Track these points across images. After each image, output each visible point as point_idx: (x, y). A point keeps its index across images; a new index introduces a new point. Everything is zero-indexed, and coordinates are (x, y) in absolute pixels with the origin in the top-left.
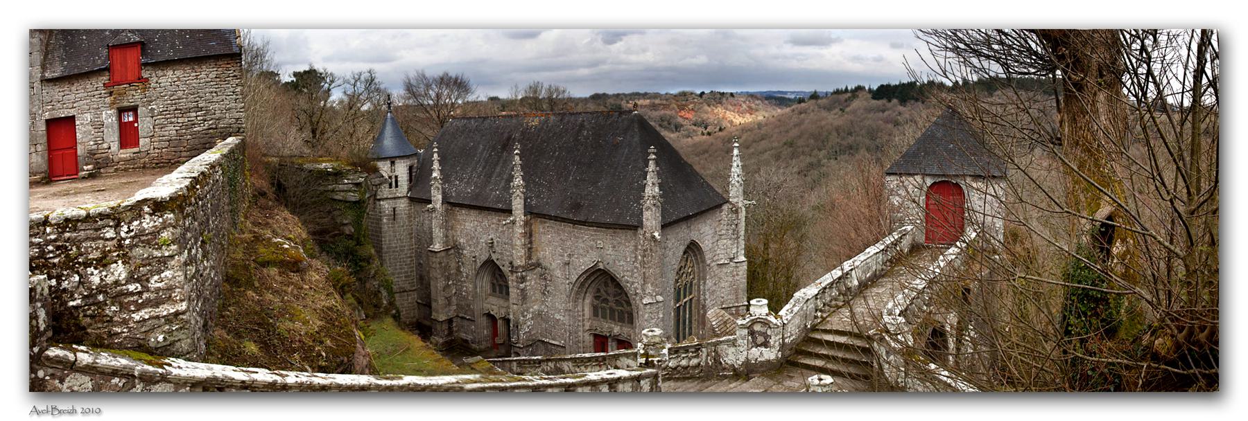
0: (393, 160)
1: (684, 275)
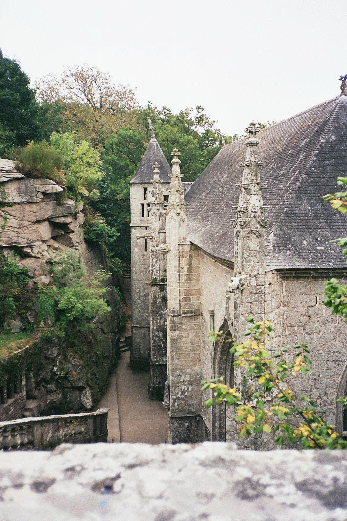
0: (146, 186)
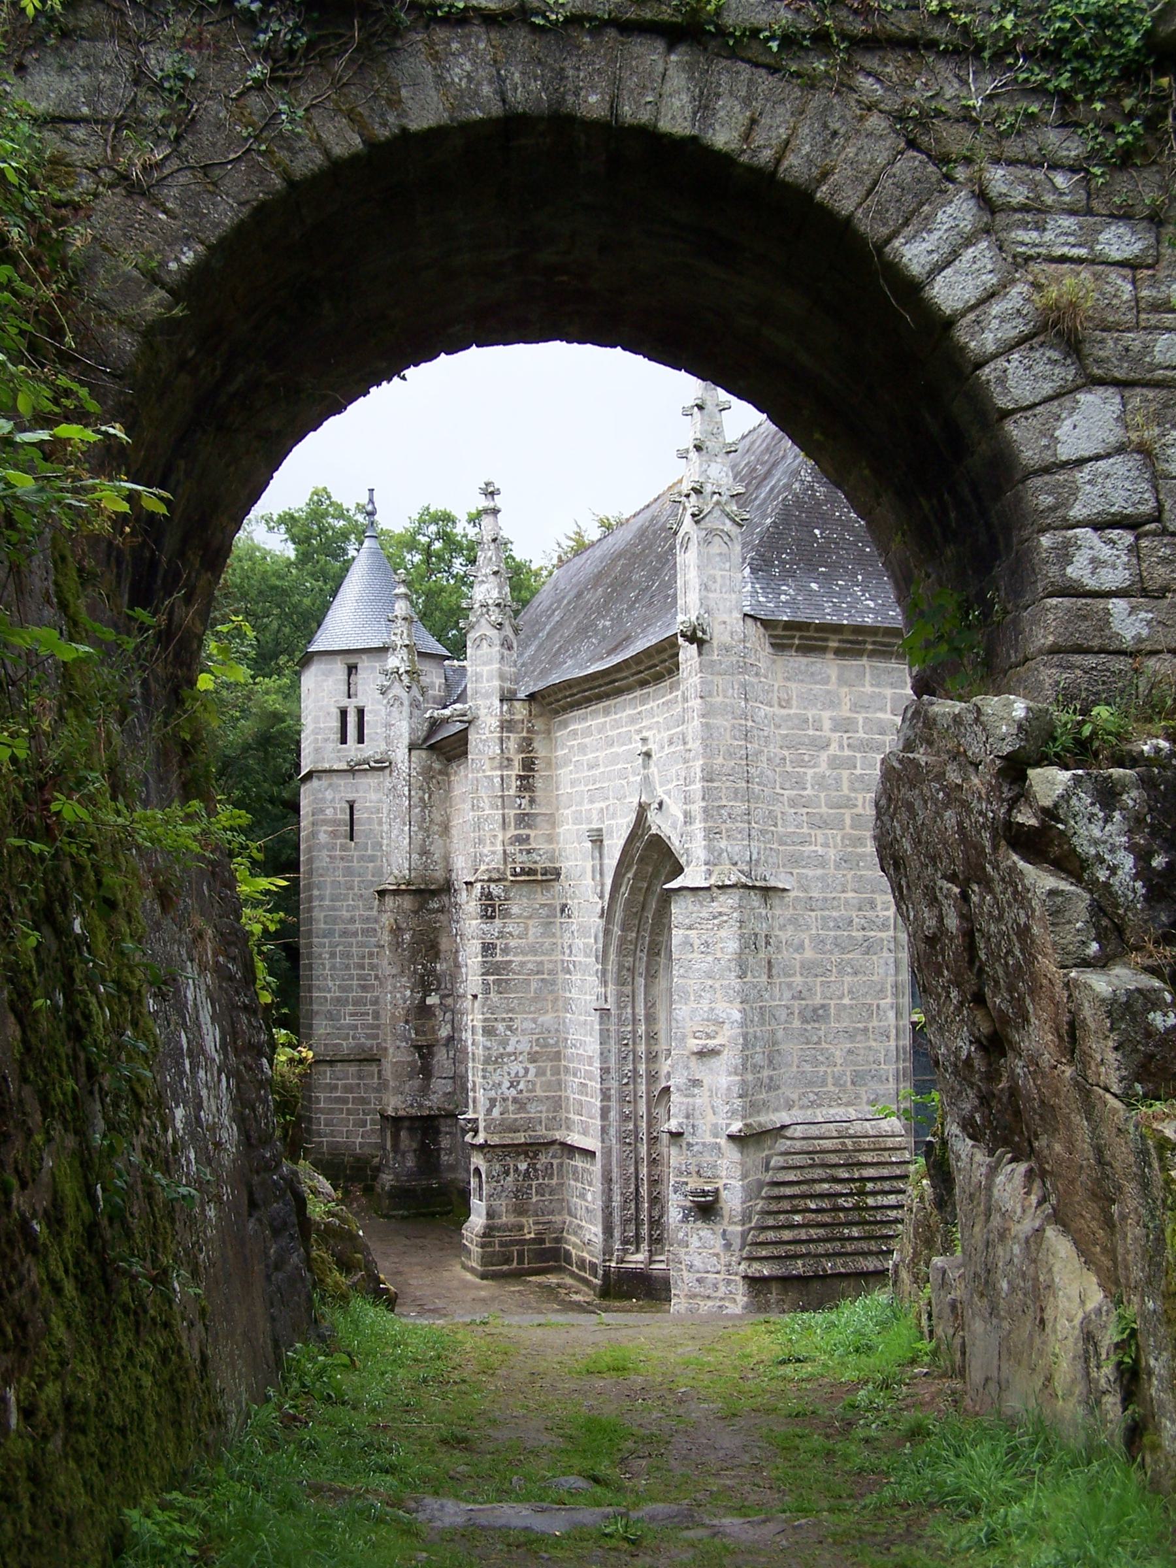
0: (352, 660)
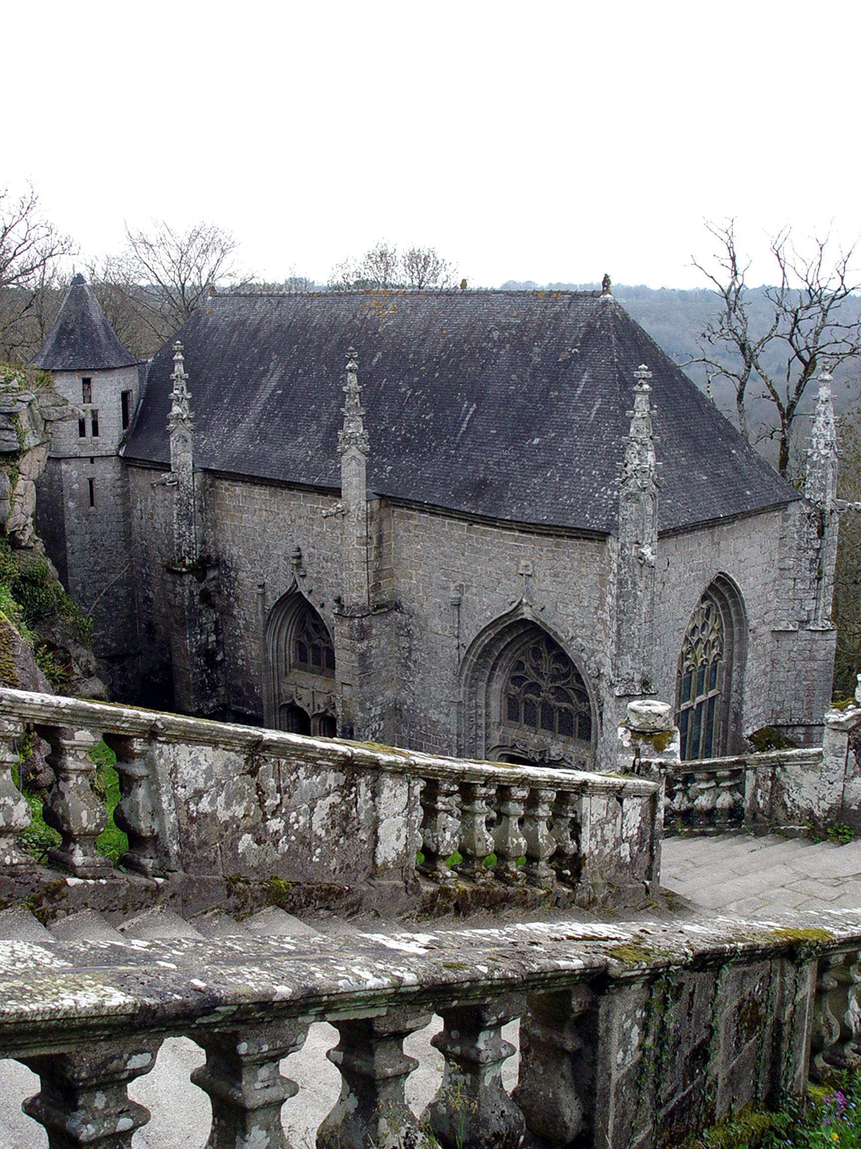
0: (87, 376)
1: (701, 646)
